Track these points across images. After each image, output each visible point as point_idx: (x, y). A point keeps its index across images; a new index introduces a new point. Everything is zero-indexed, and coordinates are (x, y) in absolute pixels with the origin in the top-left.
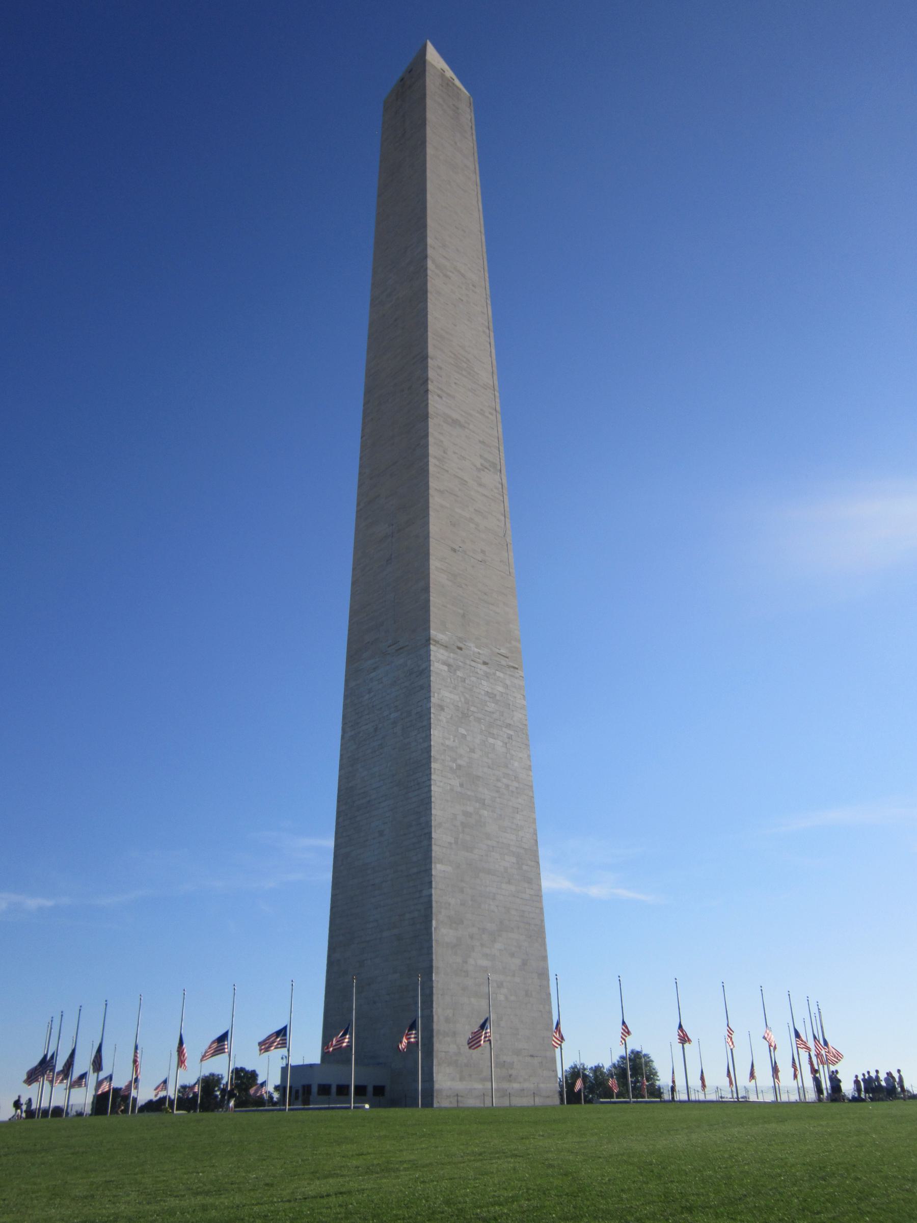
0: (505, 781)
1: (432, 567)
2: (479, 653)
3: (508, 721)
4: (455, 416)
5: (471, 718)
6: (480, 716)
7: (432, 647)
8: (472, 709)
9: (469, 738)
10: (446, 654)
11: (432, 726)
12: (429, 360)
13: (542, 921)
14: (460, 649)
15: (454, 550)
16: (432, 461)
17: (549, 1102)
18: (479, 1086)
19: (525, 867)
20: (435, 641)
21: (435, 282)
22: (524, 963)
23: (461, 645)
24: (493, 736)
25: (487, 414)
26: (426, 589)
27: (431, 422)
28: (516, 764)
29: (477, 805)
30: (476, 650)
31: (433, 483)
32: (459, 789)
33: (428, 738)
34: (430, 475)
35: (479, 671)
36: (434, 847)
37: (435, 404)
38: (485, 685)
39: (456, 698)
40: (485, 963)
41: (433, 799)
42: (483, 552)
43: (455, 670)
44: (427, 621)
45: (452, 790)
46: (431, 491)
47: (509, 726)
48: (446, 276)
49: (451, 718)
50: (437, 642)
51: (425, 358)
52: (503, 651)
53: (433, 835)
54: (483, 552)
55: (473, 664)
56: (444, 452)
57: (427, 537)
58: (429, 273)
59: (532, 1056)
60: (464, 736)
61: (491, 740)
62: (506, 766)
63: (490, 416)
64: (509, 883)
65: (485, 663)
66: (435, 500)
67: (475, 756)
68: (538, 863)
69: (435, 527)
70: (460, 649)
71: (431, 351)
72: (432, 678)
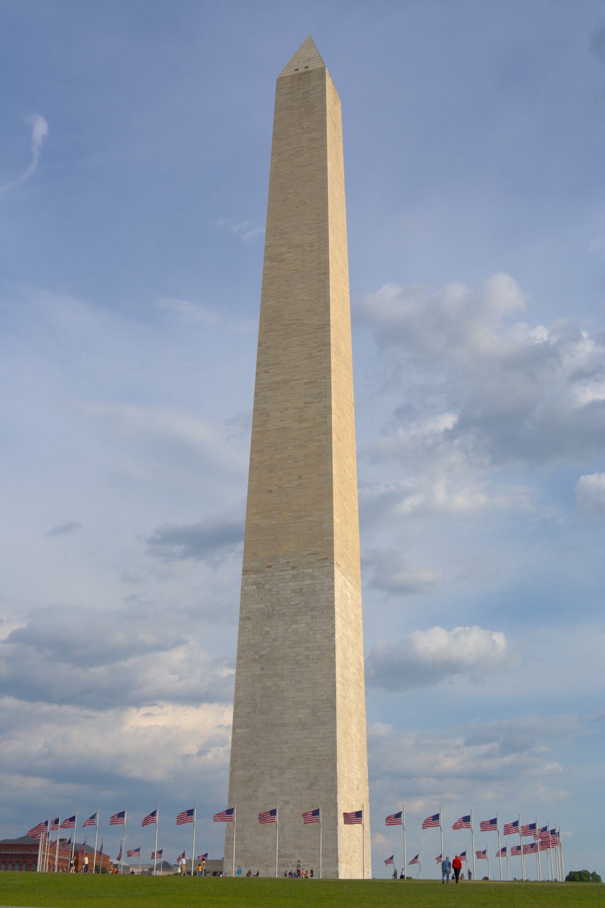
6: (284, 611)
8: (278, 608)
10: (256, 576)
14: (270, 567)
23: (269, 564)
24: (297, 622)
35: (287, 577)
39: (263, 605)
47: (312, 609)
54: (300, 477)
55: (281, 573)
60: (267, 632)
61: (294, 626)
65: (293, 568)
67: (277, 643)
68: (335, 708)
70: (270, 567)
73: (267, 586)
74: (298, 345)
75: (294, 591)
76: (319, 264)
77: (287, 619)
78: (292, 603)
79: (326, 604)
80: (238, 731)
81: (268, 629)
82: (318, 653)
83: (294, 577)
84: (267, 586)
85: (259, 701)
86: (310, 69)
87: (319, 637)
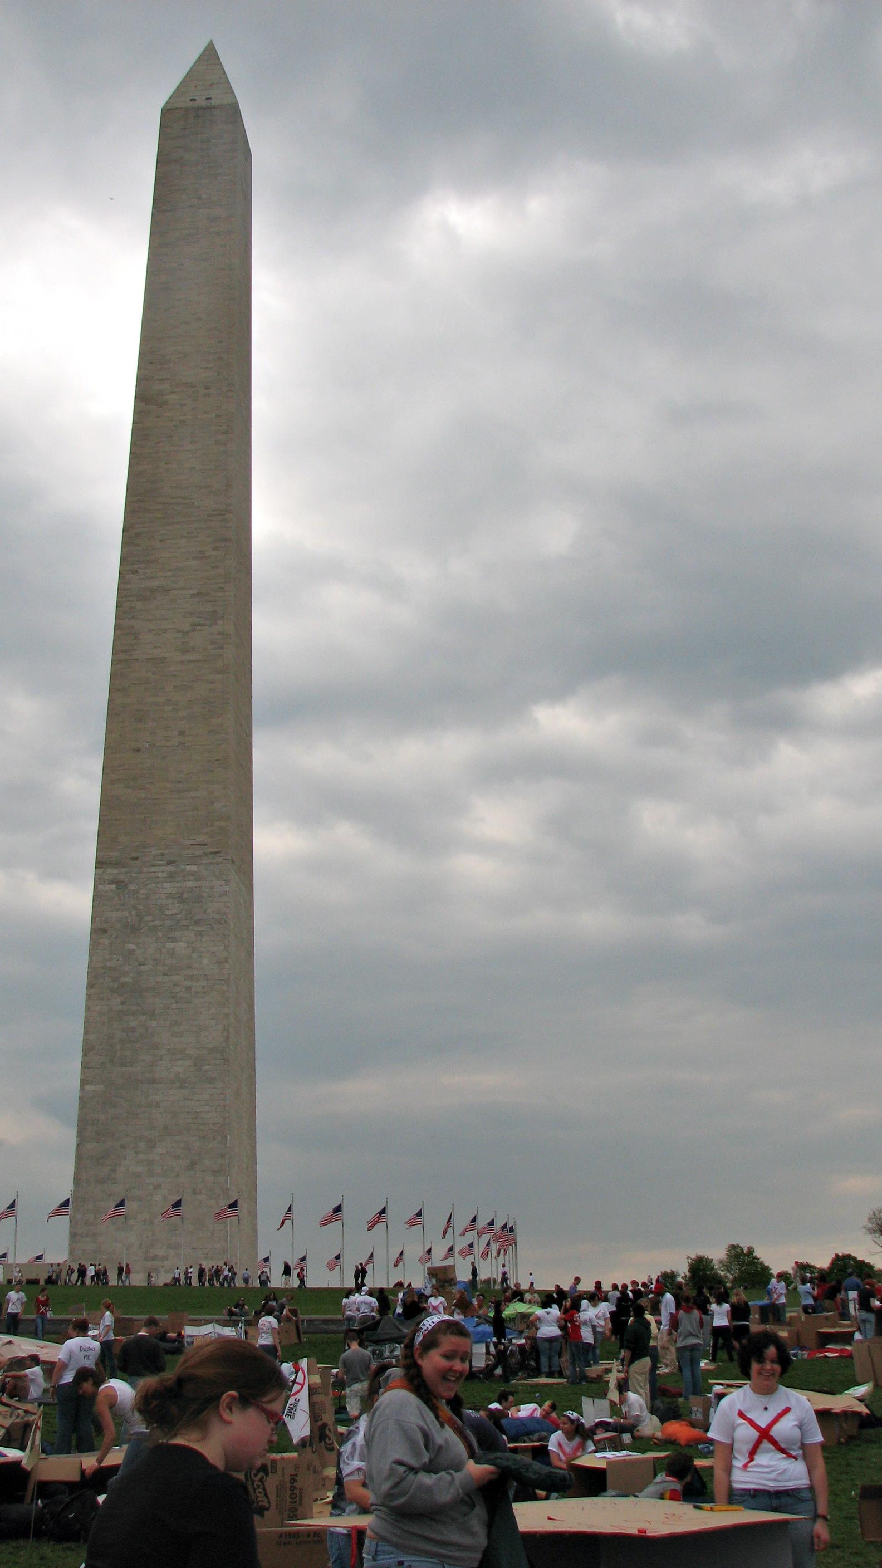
2: (163, 855)
3: (197, 917)
4: (155, 583)
6: (157, 923)
8: (149, 918)
9: (138, 952)
14: (136, 859)
15: (138, 750)
22: (193, 1165)
23: (134, 855)
24: (174, 940)
25: (207, 554)
32: (120, 1007)
35: (160, 875)
38: (169, 887)
39: (126, 913)
40: (139, 1169)
43: (126, 886)
47: (197, 923)
52: (200, 839)
54: (182, 733)
55: (153, 869)
61: (170, 945)
62: (189, 967)
63: (214, 553)
64: (181, 1087)
65: (170, 863)
70: (136, 859)
73: (131, 887)
74: (182, 537)
75: (170, 896)
76: (218, 416)
77: (160, 934)
78: (167, 912)
79: (217, 916)
80: (87, 1087)
81: (132, 946)
82: (204, 983)
83: (171, 876)
84: (131, 887)
85: (118, 1047)
86: (213, 102)
87: (205, 961)
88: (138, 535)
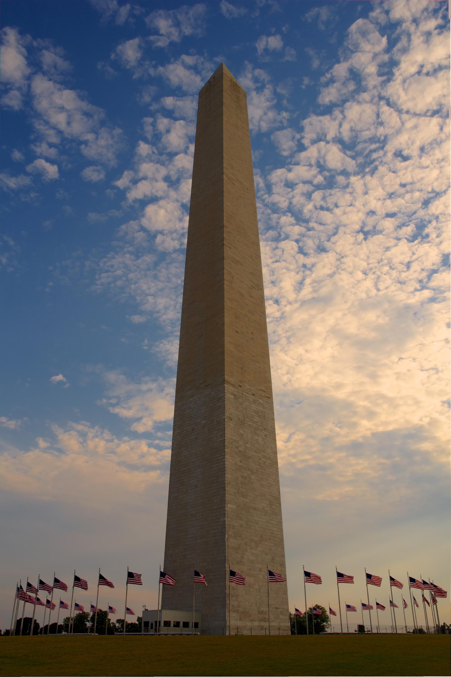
0: (263, 459)
1: (226, 341)
2: (250, 389)
5: (246, 425)
7: (226, 385)
8: (247, 419)
10: (233, 389)
11: (226, 428)
12: (224, 228)
13: (282, 536)
14: (241, 386)
16: (226, 282)
17: (282, 633)
18: (249, 624)
19: (273, 507)
20: (227, 382)
21: (227, 186)
23: (241, 384)
26: (223, 353)
27: (226, 262)
28: (269, 450)
29: (249, 472)
30: (249, 387)
31: (226, 295)
32: (240, 464)
33: (223, 435)
34: (225, 291)
36: (227, 495)
37: (228, 252)
41: (226, 469)
42: (252, 333)
43: (238, 398)
44: (223, 370)
45: (236, 464)
46: (226, 300)
47: (265, 429)
48: (233, 184)
49: (236, 424)
50: (228, 382)
51: (222, 227)
52: (262, 388)
53: (226, 488)
54: (252, 333)
55: (247, 395)
56: (232, 278)
57: (223, 324)
58: (224, 181)
59: (276, 608)
60: (242, 435)
61: (256, 437)
62: (264, 451)
65: (253, 395)
66: (227, 304)
67: (248, 446)
69: (227, 320)
70: (241, 386)
71: (225, 223)
72: (226, 402)
78: (254, 420)
81: (242, 432)
84: (240, 400)
85: (240, 485)
88: (229, 232)
